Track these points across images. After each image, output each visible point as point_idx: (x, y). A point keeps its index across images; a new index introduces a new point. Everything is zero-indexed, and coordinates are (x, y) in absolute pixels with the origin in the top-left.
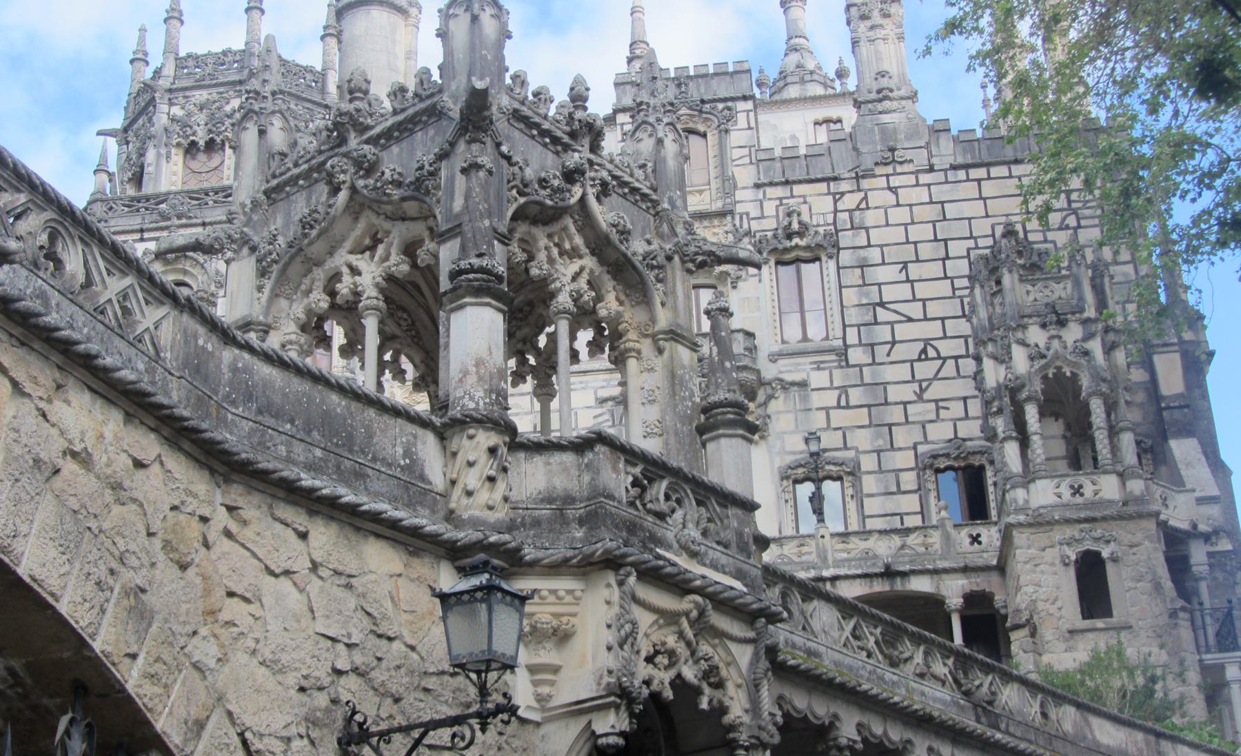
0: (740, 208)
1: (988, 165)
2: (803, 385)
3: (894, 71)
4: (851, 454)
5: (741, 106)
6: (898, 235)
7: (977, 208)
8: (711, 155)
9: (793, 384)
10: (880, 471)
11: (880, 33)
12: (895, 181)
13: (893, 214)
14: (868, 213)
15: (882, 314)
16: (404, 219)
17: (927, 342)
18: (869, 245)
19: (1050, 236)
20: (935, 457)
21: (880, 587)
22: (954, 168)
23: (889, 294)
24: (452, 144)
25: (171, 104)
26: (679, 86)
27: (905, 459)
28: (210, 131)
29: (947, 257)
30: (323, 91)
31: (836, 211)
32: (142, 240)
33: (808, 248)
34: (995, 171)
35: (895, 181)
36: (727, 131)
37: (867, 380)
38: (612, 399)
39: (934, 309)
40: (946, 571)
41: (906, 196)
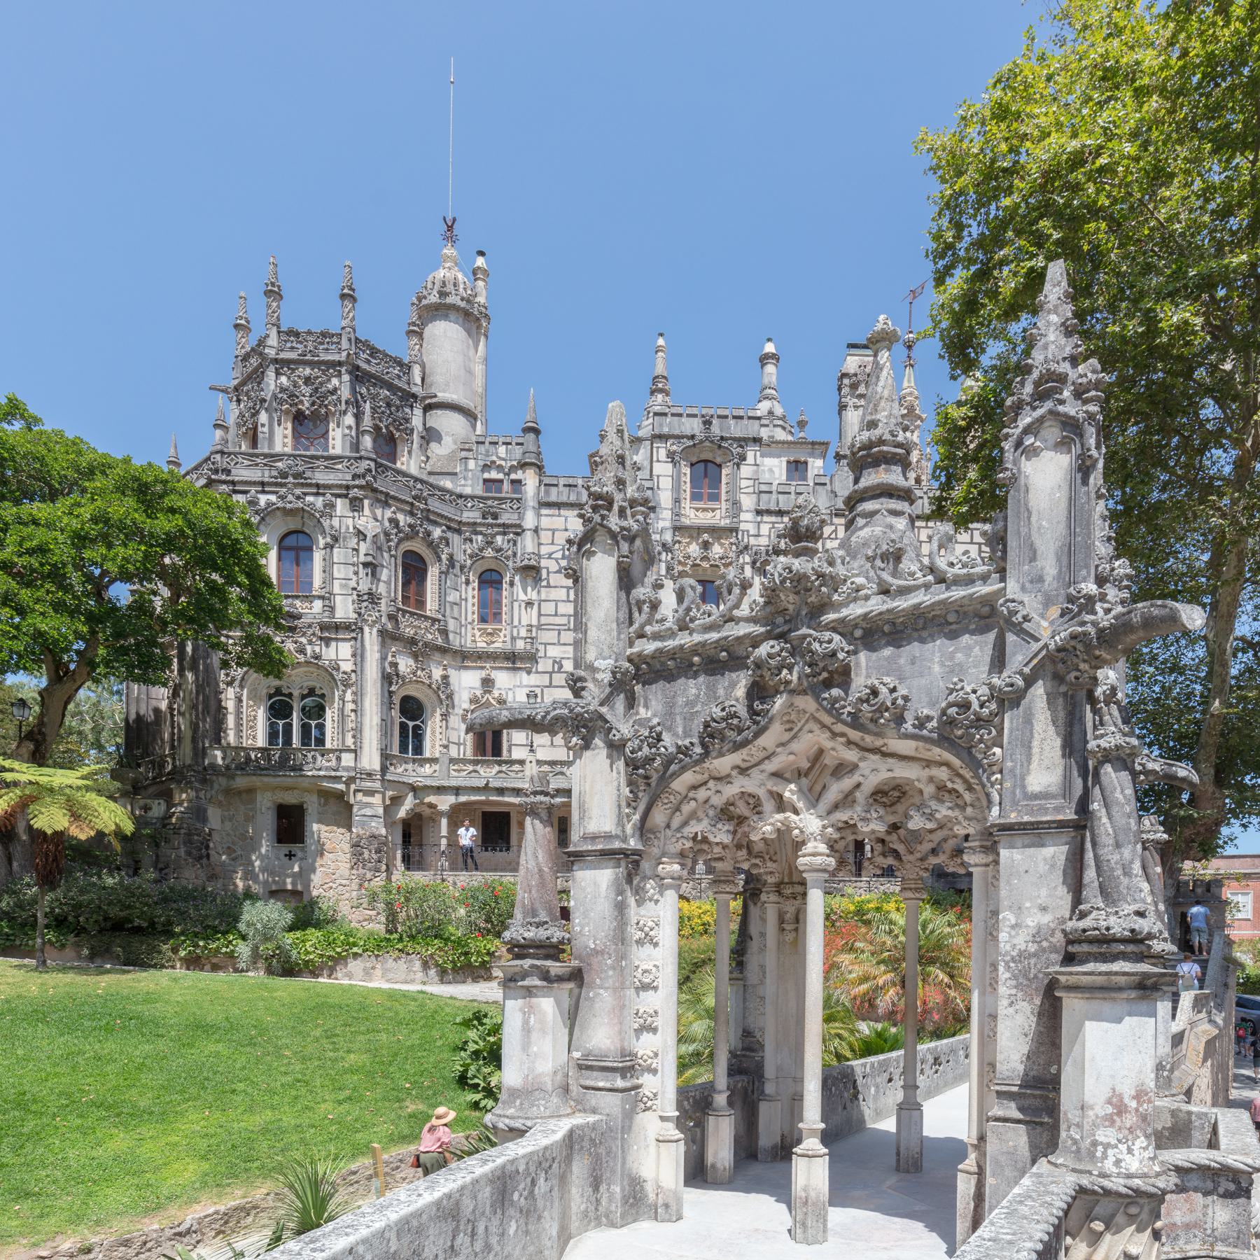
16: (885, 755)
25: (278, 374)
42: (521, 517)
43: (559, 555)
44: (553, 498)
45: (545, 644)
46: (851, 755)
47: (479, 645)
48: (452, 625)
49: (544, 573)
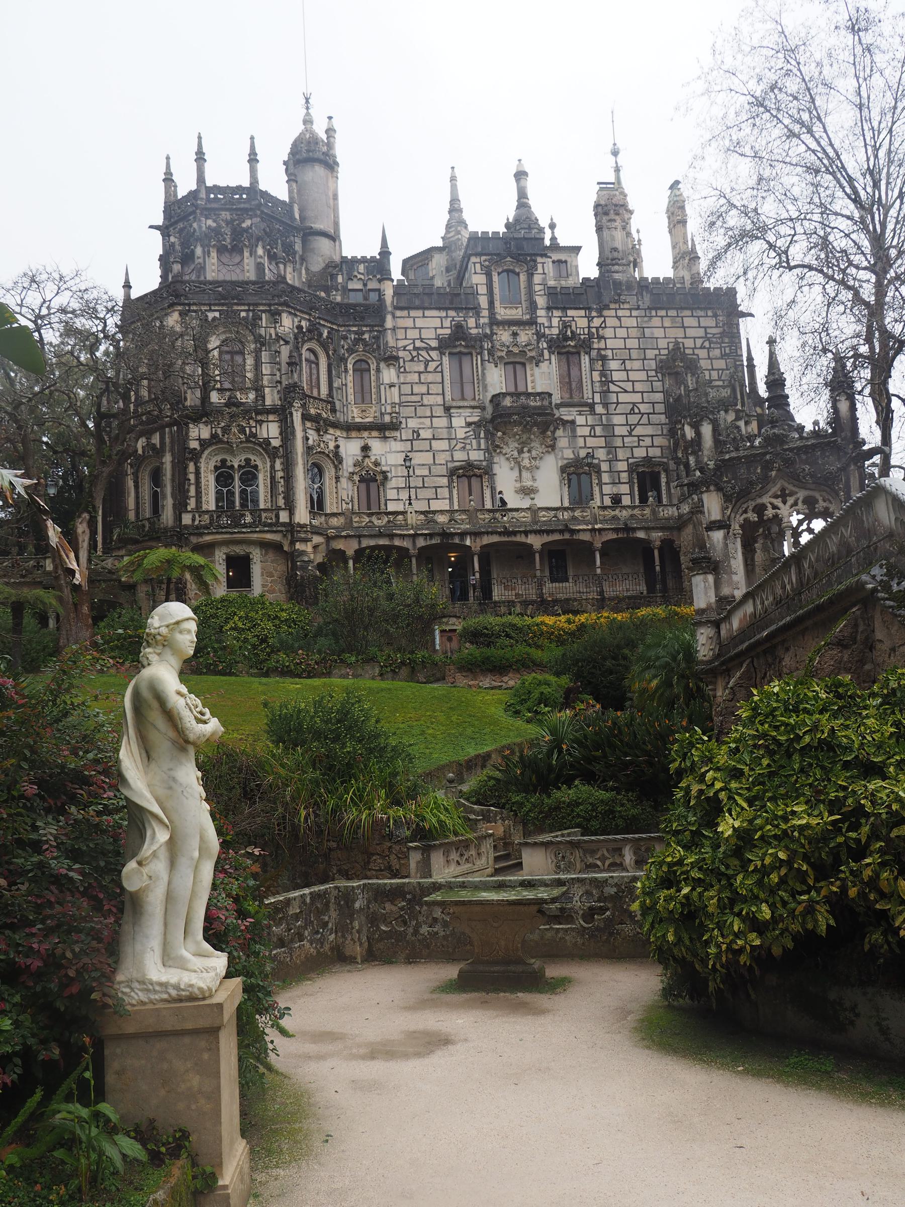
0: (539, 320)
1: (667, 309)
2: (573, 422)
3: (620, 248)
4: (596, 461)
5: (539, 260)
6: (619, 344)
7: (659, 333)
8: (522, 286)
9: (567, 421)
10: (610, 471)
11: (614, 225)
12: (620, 313)
13: (619, 330)
15: (613, 388)
17: (634, 404)
19: (696, 351)
22: (650, 309)
23: (616, 376)
24: (848, 465)
26: (506, 243)
27: (622, 466)
28: (233, 240)
29: (645, 359)
31: (589, 327)
32: (210, 310)
33: (575, 346)
35: (620, 313)
36: (532, 274)
37: (604, 422)
38: (474, 423)
39: (639, 387)
40: (653, 528)
41: (627, 322)
42: (383, 320)
43: (411, 347)
45: (406, 418)
46: (794, 489)
47: (358, 420)
48: (338, 405)
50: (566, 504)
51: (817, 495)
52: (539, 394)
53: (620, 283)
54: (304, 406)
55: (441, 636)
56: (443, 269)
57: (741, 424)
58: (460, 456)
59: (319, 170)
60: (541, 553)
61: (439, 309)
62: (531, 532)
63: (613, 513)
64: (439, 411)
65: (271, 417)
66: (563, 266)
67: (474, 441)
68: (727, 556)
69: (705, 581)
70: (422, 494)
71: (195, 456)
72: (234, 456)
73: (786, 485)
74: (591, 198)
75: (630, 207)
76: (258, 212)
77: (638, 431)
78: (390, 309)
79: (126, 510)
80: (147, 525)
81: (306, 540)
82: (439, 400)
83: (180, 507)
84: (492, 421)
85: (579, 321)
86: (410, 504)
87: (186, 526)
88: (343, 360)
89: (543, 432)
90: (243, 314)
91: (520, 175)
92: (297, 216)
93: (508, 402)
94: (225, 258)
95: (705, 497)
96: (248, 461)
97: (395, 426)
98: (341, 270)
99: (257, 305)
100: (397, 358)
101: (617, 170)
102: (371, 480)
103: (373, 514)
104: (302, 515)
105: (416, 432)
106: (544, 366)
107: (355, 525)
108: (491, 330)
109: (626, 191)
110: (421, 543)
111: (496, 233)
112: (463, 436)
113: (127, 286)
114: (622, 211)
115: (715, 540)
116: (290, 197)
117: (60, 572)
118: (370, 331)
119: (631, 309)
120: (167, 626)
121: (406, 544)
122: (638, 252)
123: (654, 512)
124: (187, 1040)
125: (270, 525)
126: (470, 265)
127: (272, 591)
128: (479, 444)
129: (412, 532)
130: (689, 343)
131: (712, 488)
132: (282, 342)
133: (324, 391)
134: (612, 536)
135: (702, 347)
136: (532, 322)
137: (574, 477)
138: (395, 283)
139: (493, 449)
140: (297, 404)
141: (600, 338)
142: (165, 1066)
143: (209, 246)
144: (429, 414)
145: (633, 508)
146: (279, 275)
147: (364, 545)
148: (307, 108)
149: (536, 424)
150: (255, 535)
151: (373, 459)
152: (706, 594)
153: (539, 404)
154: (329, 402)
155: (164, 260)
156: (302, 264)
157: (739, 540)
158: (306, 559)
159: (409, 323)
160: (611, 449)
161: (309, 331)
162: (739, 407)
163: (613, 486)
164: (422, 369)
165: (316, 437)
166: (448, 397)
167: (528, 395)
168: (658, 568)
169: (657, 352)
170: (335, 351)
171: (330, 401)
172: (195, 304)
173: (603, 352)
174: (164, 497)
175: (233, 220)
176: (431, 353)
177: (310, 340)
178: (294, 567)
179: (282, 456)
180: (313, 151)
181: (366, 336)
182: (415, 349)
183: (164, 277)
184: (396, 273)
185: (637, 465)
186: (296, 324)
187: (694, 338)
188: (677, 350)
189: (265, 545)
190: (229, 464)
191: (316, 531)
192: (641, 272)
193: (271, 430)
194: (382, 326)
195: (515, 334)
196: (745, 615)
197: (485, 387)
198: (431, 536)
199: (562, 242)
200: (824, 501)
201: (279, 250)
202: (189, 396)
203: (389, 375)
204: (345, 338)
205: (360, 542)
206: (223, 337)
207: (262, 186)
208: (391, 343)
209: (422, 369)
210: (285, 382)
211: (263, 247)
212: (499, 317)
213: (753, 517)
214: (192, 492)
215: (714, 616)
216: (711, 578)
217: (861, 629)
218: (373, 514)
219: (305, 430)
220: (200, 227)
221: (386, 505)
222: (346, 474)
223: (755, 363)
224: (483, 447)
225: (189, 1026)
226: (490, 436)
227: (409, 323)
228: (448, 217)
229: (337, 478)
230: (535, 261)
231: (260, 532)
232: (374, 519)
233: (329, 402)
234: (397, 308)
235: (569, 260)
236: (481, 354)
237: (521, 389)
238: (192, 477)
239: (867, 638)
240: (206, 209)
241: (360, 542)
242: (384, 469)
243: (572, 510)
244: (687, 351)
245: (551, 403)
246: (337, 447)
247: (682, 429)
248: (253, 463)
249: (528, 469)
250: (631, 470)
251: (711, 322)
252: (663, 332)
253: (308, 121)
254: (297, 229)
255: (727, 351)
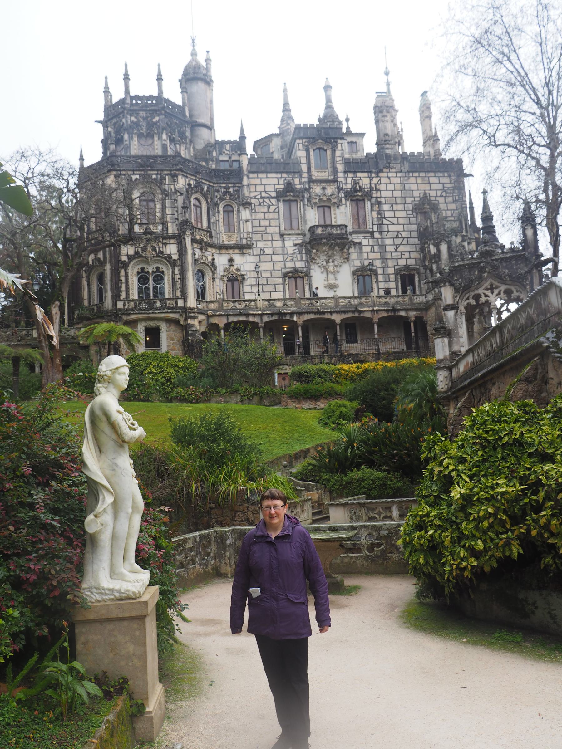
0: (339, 179)
1: (419, 172)
2: (360, 243)
3: (390, 133)
4: (374, 268)
5: (339, 141)
6: (389, 194)
9: (357, 243)
10: (384, 274)
11: (386, 119)
13: (389, 185)
14: (381, 185)
17: (398, 232)
18: (381, 197)
19: (437, 199)
20: (401, 270)
21: (390, 314)
22: (408, 172)
23: (387, 214)
24: (532, 269)
26: (318, 131)
27: (391, 271)
28: (147, 129)
29: (405, 203)
30: (184, 115)
31: (370, 184)
32: (134, 174)
33: (362, 196)
34: (422, 174)
37: (380, 243)
39: (401, 221)
40: (410, 309)
42: (241, 180)
43: (259, 197)
44: (253, 170)
45: (256, 241)
46: (498, 284)
47: (226, 243)
48: (214, 233)
49: (253, 205)
50: (356, 294)
51: (513, 288)
52: (339, 226)
53: (390, 156)
54: (192, 234)
55: (279, 377)
56: (279, 147)
57: (465, 244)
58: (290, 265)
59: (201, 85)
60: (340, 325)
61: (277, 172)
62: (334, 312)
63: (385, 300)
64: (277, 237)
65: (172, 241)
66: (354, 145)
67: (299, 256)
68: (456, 326)
69: (443, 342)
70: (266, 288)
71: (125, 265)
72: (149, 265)
73: (493, 282)
74: (372, 102)
75: (396, 107)
76: (163, 112)
77: (401, 248)
78: (246, 173)
79: (82, 299)
80: (96, 308)
81: (194, 318)
82: (277, 230)
83: (116, 297)
84: (310, 243)
85: (364, 180)
86: (259, 295)
87: (120, 310)
88: (217, 205)
89: (342, 250)
90: (154, 176)
91: (327, 88)
92: (187, 114)
93: (319, 231)
94: (143, 141)
95: (443, 290)
96: (158, 268)
97: (249, 246)
98: (215, 148)
99: (162, 170)
100: (250, 204)
101: (388, 84)
102: (235, 280)
103: (236, 301)
104: (192, 302)
105: (262, 250)
106: (342, 208)
107: (225, 308)
108: (309, 186)
109: (394, 98)
110: (266, 319)
111: (312, 125)
112: (292, 252)
113: (82, 159)
114: (391, 110)
115: (449, 316)
116: (183, 103)
117: (42, 338)
118: (234, 187)
119: (396, 172)
120: (111, 370)
121: (257, 320)
122: (401, 136)
123: (411, 299)
124: (126, 623)
125: (172, 308)
126: (296, 145)
127: (173, 350)
128: (302, 257)
129: (260, 312)
130: (433, 193)
131: (447, 284)
132: (178, 194)
133: (205, 224)
134: (385, 314)
135: (441, 196)
136: (335, 181)
137: (361, 278)
138: (249, 156)
139: (311, 260)
140: (188, 233)
141: (377, 190)
142: (113, 639)
143: (132, 133)
144: (270, 239)
145: (398, 296)
146: (177, 152)
147: (230, 320)
148: (194, 46)
149: (337, 244)
150: (163, 315)
151: (236, 267)
152: (443, 350)
153: (339, 232)
154: (207, 231)
155: (105, 143)
156: (190, 145)
157: (464, 316)
158: (194, 329)
159: (258, 181)
160: (384, 260)
161: (195, 187)
162: (464, 233)
163: (385, 282)
164: (265, 210)
165: (200, 254)
166: (282, 228)
167: (332, 226)
168: (413, 334)
169: (413, 199)
170: (211, 199)
171: (209, 231)
172: (124, 170)
173: (379, 200)
174: (106, 291)
175: (147, 117)
176: (272, 200)
177: (196, 192)
178: (187, 334)
179: (179, 265)
180: (197, 73)
181: (231, 190)
182: (262, 198)
183: (105, 153)
184: (250, 150)
185: (400, 270)
186: (187, 182)
187: (436, 190)
188: (425, 198)
189: (169, 321)
190: (146, 270)
191: (201, 312)
192: (403, 149)
193: (172, 249)
194: (241, 183)
195: (324, 188)
196: (467, 363)
197: (305, 222)
198: (272, 314)
199: (353, 130)
200: (517, 292)
201: (176, 136)
202: (121, 228)
203: (245, 214)
204: (218, 191)
205: (228, 319)
206: (142, 191)
207: (166, 96)
208: (247, 194)
209: (265, 210)
210: (181, 219)
211: (167, 134)
212: (314, 178)
213: (473, 302)
214: (123, 288)
215: (448, 364)
216: (446, 340)
217: (539, 371)
218: (236, 301)
219: (193, 249)
220: (127, 121)
221: (244, 295)
222: (219, 276)
223: (474, 205)
224: (304, 259)
225: (127, 615)
226: (308, 252)
227: (258, 181)
228: (282, 114)
229: (214, 279)
230: (336, 142)
231: (166, 312)
232: (236, 304)
233: (207, 231)
234: (250, 172)
235: (358, 141)
236: (303, 200)
237: (328, 223)
238: (123, 279)
239: (543, 377)
240: (130, 110)
241: (228, 319)
242: (243, 273)
243: (360, 298)
244: (432, 199)
245: (346, 231)
246: (213, 259)
247: (429, 247)
248: (161, 270)
249: (332, 273)
250: (397, 273)
251: (446, 180)
252: (417, 186)
253: (194, 54)
254: (187, 122)
255: (457, 198)
